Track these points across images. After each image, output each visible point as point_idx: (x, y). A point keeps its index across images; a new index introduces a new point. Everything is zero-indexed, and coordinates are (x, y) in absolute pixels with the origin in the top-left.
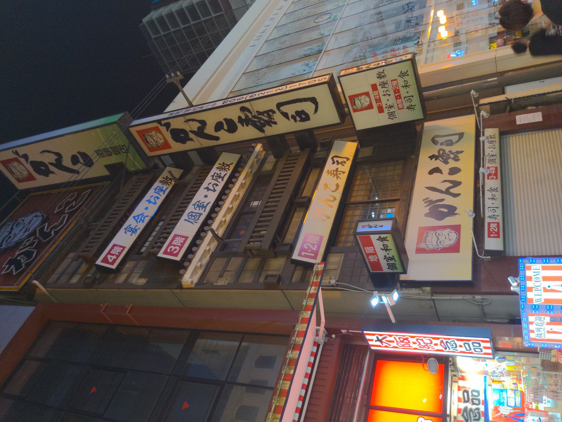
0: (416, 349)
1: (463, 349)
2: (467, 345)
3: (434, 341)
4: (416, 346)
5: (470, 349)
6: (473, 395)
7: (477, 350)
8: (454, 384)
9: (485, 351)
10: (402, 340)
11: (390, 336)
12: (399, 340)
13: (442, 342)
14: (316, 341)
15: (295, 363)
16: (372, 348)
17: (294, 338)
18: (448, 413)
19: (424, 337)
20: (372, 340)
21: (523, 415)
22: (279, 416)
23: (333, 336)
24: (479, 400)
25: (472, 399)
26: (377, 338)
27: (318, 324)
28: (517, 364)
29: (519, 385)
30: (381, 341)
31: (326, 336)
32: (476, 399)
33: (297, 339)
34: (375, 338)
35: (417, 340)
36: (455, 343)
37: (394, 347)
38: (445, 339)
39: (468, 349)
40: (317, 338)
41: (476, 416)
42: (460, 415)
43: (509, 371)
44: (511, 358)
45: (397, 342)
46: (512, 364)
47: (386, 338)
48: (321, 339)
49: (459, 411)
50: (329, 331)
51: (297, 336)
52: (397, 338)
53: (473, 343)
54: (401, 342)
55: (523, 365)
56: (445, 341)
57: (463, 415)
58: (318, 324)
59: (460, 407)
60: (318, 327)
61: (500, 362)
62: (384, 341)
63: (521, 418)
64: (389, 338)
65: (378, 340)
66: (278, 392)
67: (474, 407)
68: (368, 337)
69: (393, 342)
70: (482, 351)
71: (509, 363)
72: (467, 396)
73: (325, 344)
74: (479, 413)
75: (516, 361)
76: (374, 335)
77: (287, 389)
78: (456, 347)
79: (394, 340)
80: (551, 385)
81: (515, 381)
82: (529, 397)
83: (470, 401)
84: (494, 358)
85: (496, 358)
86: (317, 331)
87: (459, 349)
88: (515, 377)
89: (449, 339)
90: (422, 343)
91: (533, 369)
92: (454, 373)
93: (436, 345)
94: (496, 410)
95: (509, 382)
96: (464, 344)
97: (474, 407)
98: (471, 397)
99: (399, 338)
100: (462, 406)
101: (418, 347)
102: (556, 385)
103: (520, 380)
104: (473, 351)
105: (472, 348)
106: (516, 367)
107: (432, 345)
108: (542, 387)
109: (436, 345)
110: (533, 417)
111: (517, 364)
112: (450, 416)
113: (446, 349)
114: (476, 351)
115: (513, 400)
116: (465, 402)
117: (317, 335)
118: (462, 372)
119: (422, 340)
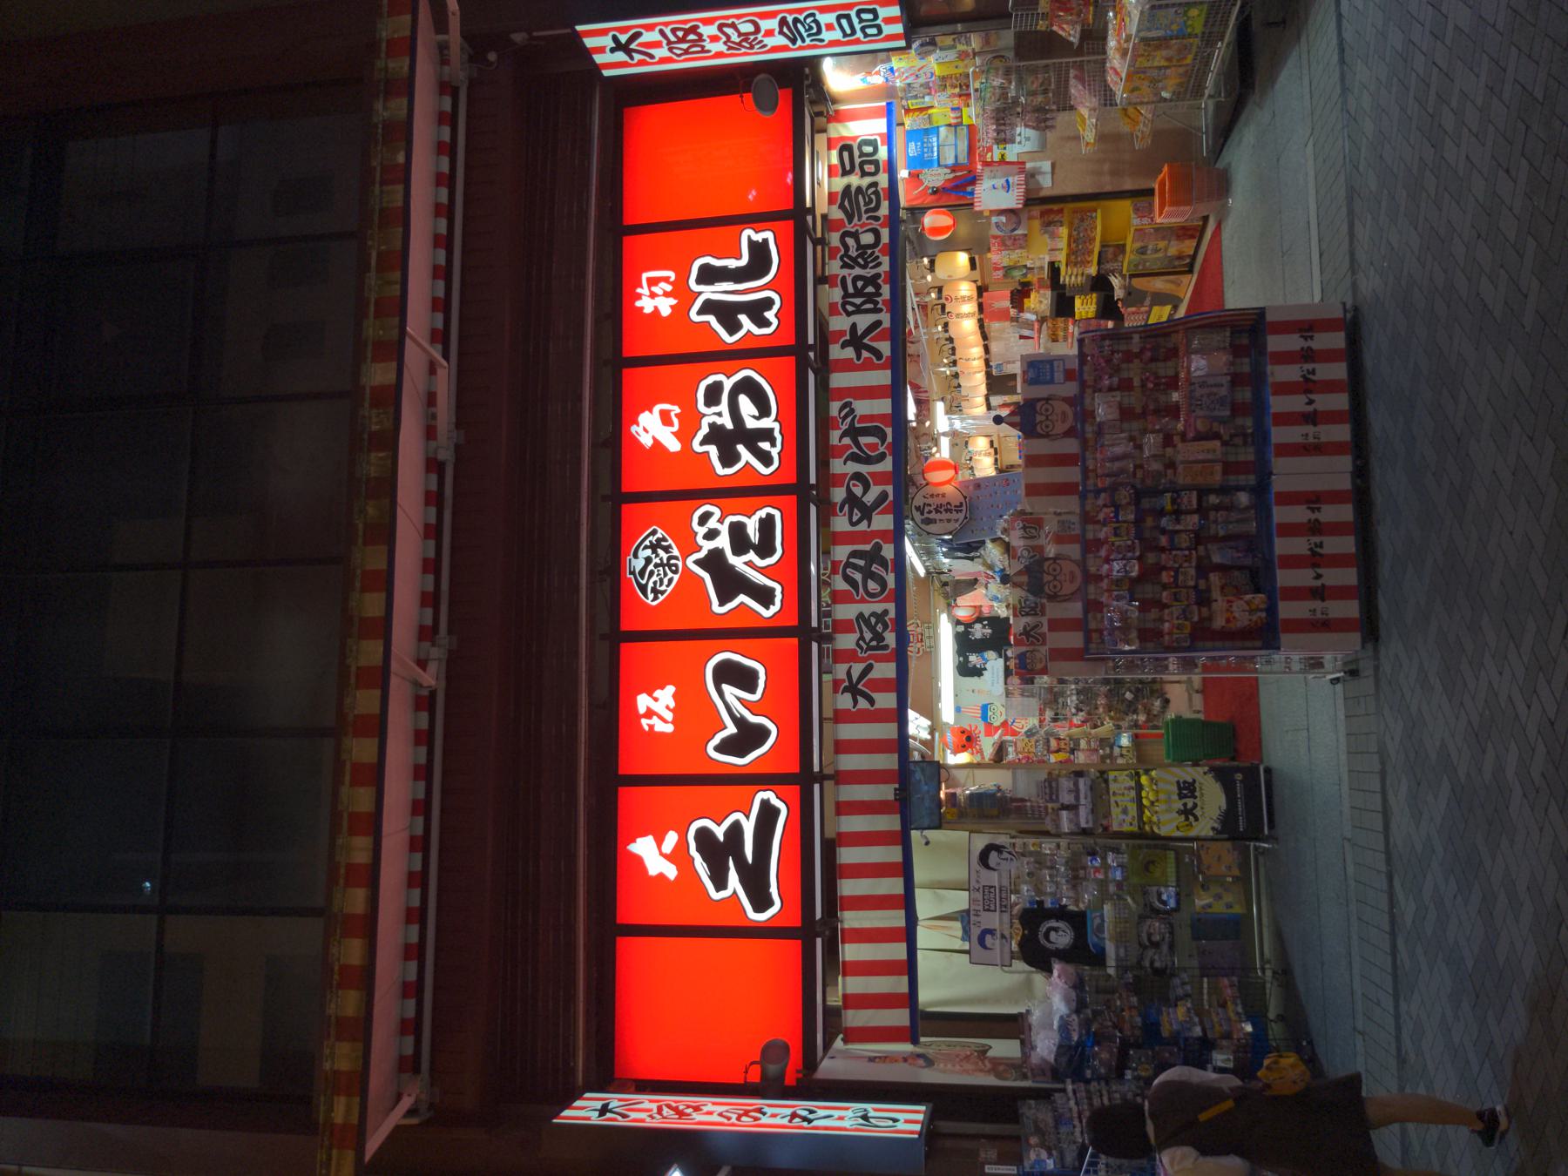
0: (719, 55)
1: (836, 35)
2: (844, 22)
3: (766, 25)
4: (719, 47)
5: (854, 32)
6: (862, 154)
7: (869, 31)
8: (817, 136)
9: (888, 30)
10: (680, 34)
11: (650, 28)
12: (673, 39)
13: (783, 22)
14: (446, 79)
15: (402, 132)
16: (606, 73)
17: (380, 64)
18: (808, 204)
19: (738, 17)
20: (601, 50)
21: (973, 180)
22: (397, 275)
23: (492, 57)
24: (876, 163)
25: (862, 164)
26: (615, 39)
27: (441, 24)
28: (963, 56)
29: (965, 110)
30: (629, 52)
31: (471, 59)
32: (870, 162)
33: (391, 65)
34: (607, 41)
35: (720, 28)
36: (816, 22)
37: (663, 61)
38: (790, 12)
39: (848, 31)
40: (446, 69)
41: (871, 201)
42: (835, 207)
43: (943, 78)
44: (948, 40)
45: (669, 43)
46: (951, 55)
47: (638, 35)
48: (459, 71)
49: (832, 197)
50: (477, 45)
51: (388, 55)
52: (668, 31)
53: (859, 13)
54: (680, 40)
55: (975, 54)
56: (790, 19)
57: (841, 206)
58: (441, 24)
59: (834, 190)
60: (440, 37)
61: (922, 55)
62: (633, 46)
63: (969, 189)
64: (648, 37)
65: (619, 46)
66: (376, 218)
67: (867, 180)
68: (590, 42)
69: (657, 45)
70: (880, 31)
71: (943, 54)
72: (852, 157)
73: (472, 84)
74: (876, 193)
75: (960, 47)
76: (604, 32)
77: (400, 204)
78: (819, 32)
79: (659, 38)
80: (1034, 93)
81: (956, 101)
82: (987, 133)
83: (857, 169)
84: (909, 47)
85: (914, 46)
86: (443, 48)
87: (827, 36)
88: (957, 90)
89: (800, 11)
90: (735, 38)
91: (997, 63)
92: (817, 109)
93: (770, 33)
94: (915, 177)
95: (941, 108)
96: (839, 18)
97: (867, 180)
98: (857, 161)
99: (674, 31)
100: (840, 183)
101: (723, 48)
102: (1045, 92)
103: (969, 95)
104: (859, 35)
105: (858, 27)
106: (961, 64)
107: (760, 37)
108: (1016, 102)
109: (770, 33)
110: (994, 182)
111: (963, 56)
112: (812, 210)
113: (794, 41)
114: (866, 35)
115: (950, 149)
116: (845, 173)
117: (444, 61)
118: (834, 101)
119: (733, 26)
